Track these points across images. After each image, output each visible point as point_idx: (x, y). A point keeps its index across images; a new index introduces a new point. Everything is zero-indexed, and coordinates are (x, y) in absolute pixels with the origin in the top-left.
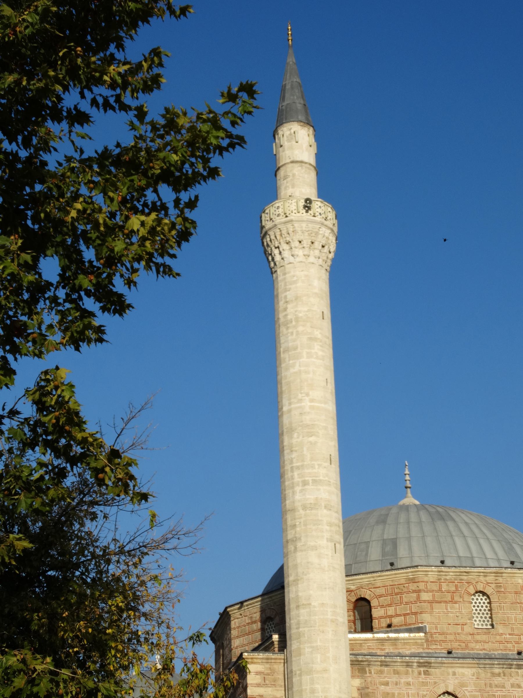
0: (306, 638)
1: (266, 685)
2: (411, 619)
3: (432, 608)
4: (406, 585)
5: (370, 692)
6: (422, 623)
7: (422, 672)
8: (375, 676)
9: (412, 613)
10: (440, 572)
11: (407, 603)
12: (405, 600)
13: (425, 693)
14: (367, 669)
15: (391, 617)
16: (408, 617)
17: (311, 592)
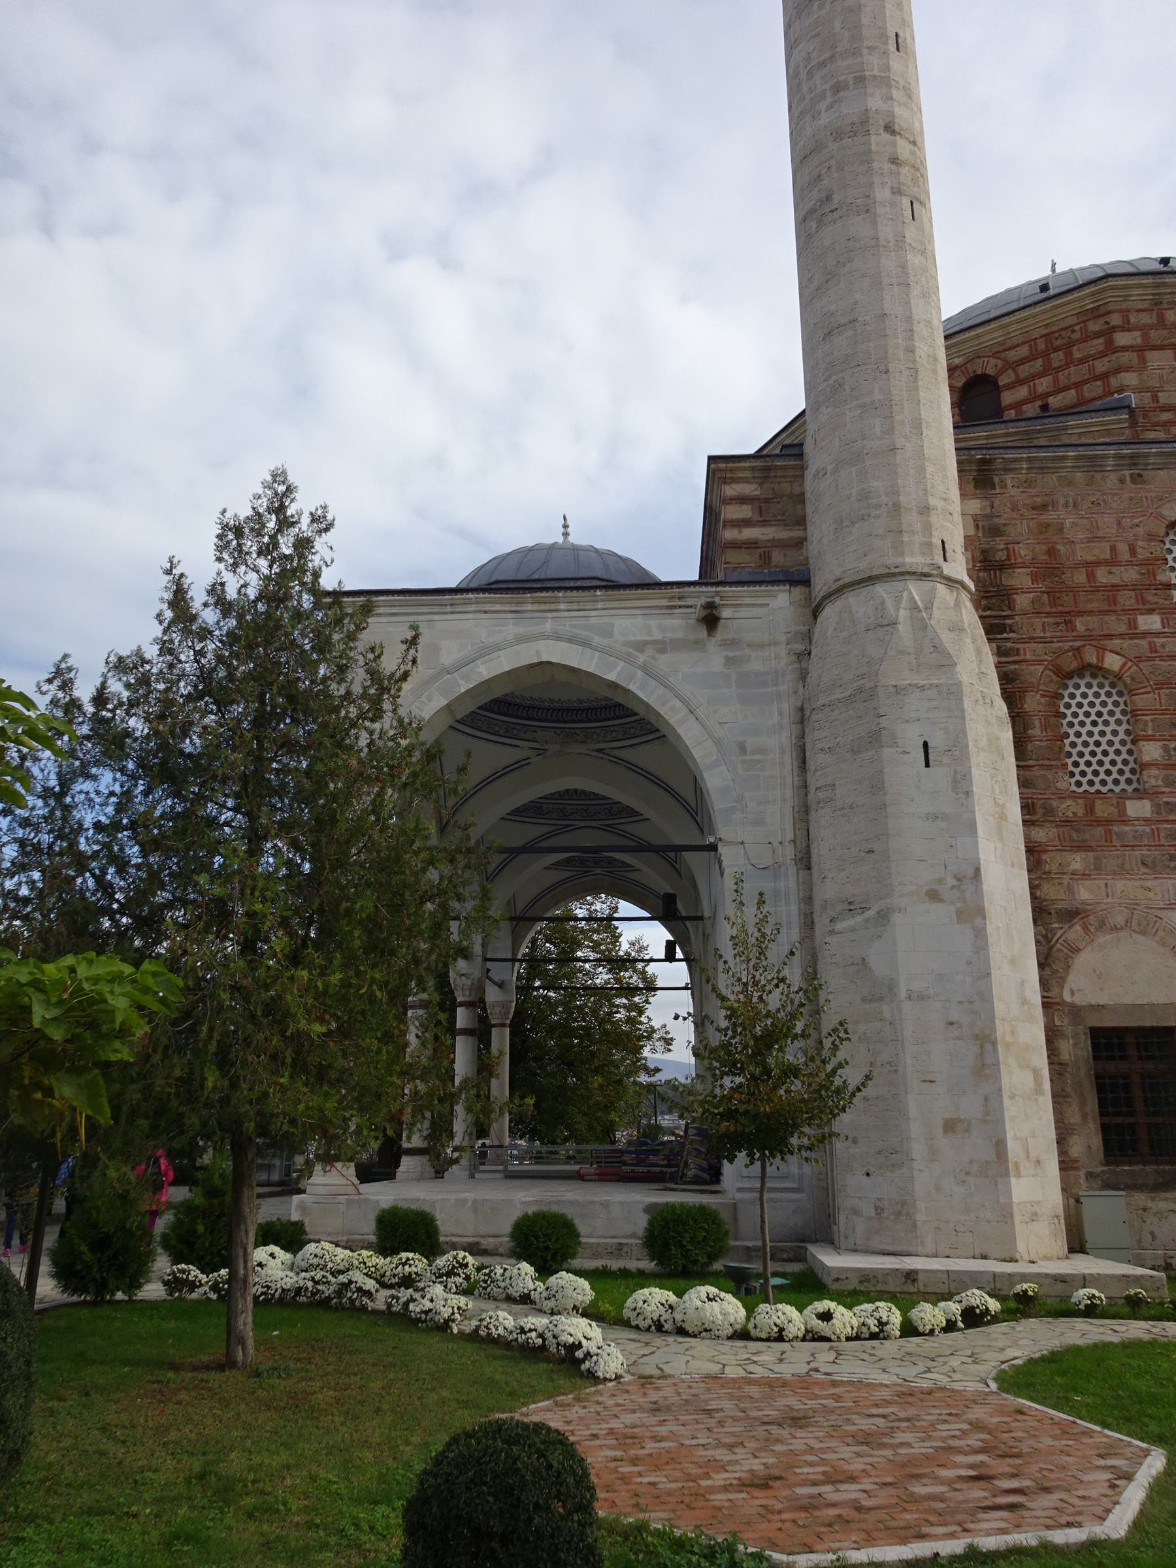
0: (848, 391)
1: (764, 523)
2: (1093, 389)
3: (1143, 361)
4: (1077, 328)
5: (1005, 525)
6: (1120, 391)
7: (1128, 479)
8: (1014, 492)
9: (1096, 378)
10: (1157, 286)
11: (1081, 361)
12: (1077, 355)
13: (1137, 521)
14: (996, 479)
15: (1047, 395)
16: (1086, 388)
17: (858, 296)
